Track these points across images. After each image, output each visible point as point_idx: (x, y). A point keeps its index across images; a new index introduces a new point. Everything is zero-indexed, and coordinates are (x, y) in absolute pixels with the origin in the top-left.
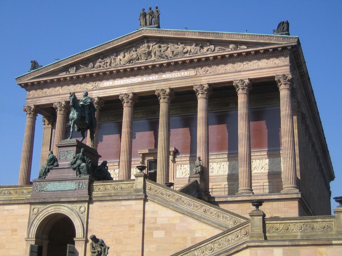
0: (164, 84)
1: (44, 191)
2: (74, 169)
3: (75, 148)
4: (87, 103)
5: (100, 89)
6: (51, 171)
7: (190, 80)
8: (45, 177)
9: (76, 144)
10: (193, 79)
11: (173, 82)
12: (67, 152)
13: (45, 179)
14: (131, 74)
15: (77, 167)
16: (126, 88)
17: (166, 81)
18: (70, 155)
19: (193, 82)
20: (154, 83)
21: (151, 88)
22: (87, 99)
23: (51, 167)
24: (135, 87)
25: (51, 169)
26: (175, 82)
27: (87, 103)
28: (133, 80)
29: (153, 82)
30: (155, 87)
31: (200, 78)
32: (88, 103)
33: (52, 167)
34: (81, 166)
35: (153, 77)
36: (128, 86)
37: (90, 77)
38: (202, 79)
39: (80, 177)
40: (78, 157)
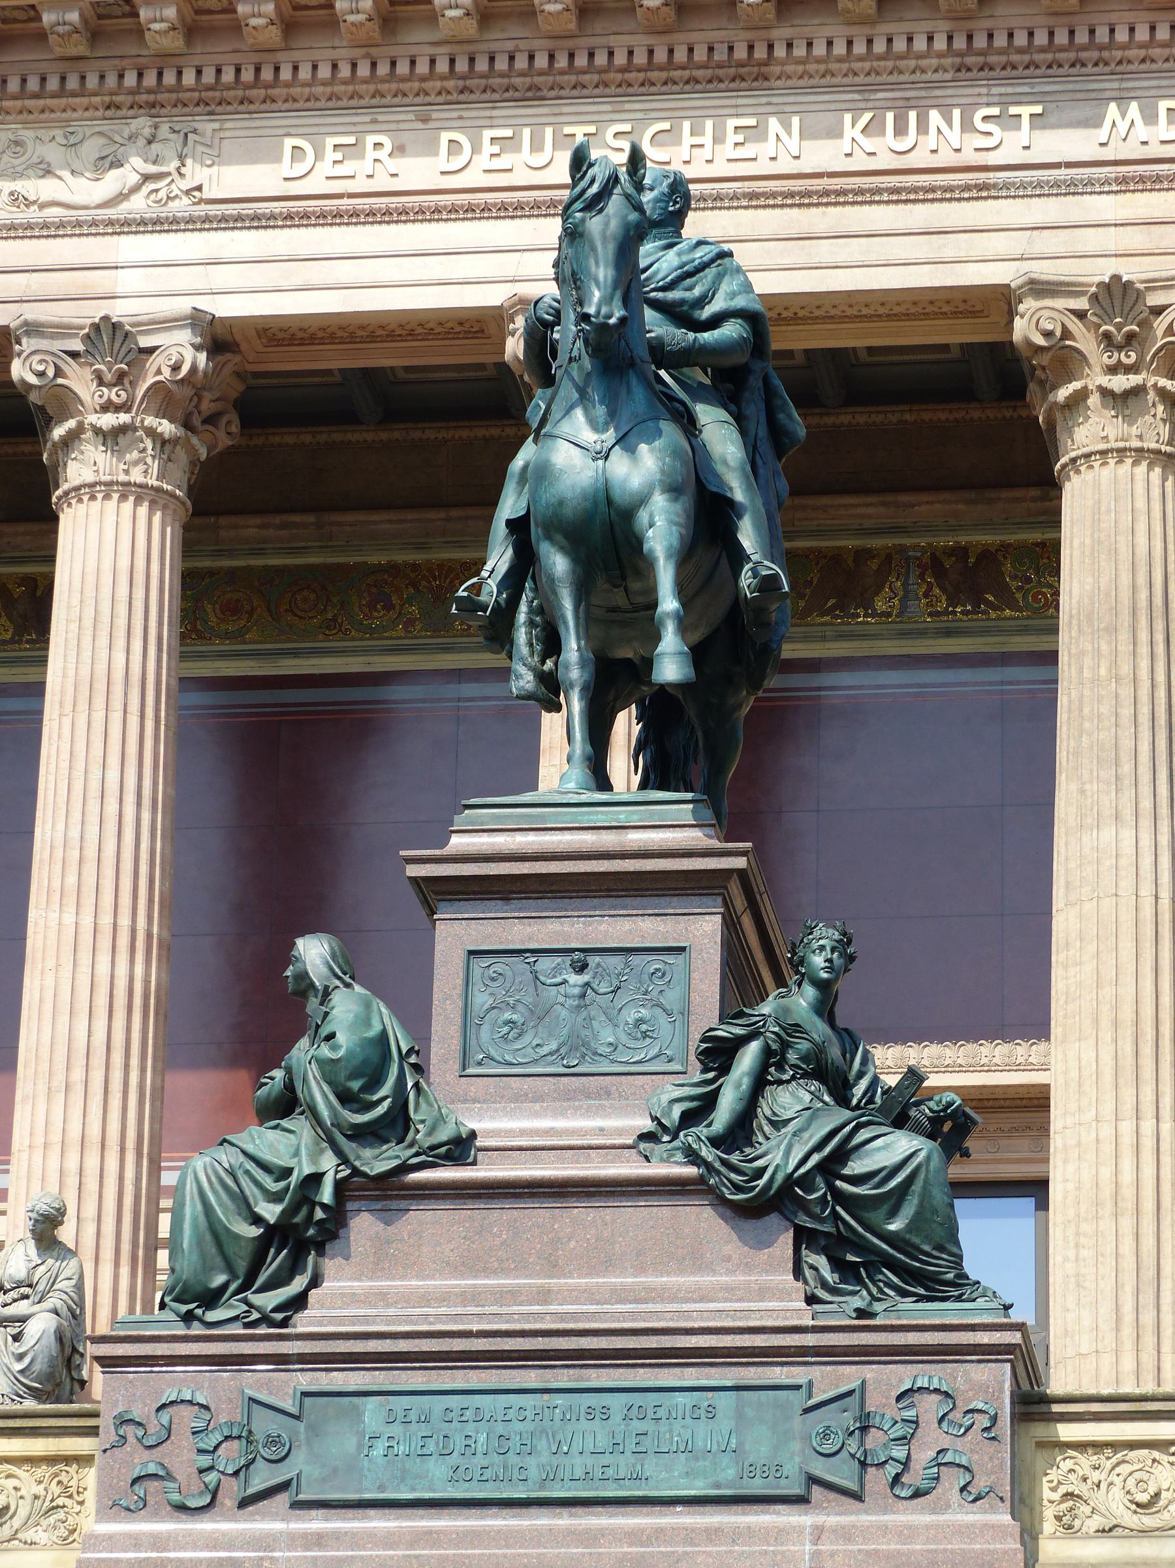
0: (1123, 214)
1: (297, 1505)
2: (756, 1207)
3: (703, 931)
4: (715, 322)
5: (215, 210)
6: (363, 1225)
8: (299, 1302)
9: (740, 863)
12: (581, 968)
13: (303, 1322)
14: (661, 56)
15: (806, 1182)
18: (631, 1015)
20: (983, 192)
22: (710, 273)
23: (377, 1160)
25: (390, 1191)
27: (715, 322)
28: (687, 140)
32: (731, 330)
33: (404, 1168)
34: (855, 1167)
37: (82, 50)
39: (861, 1313)
40: (785, 1045)
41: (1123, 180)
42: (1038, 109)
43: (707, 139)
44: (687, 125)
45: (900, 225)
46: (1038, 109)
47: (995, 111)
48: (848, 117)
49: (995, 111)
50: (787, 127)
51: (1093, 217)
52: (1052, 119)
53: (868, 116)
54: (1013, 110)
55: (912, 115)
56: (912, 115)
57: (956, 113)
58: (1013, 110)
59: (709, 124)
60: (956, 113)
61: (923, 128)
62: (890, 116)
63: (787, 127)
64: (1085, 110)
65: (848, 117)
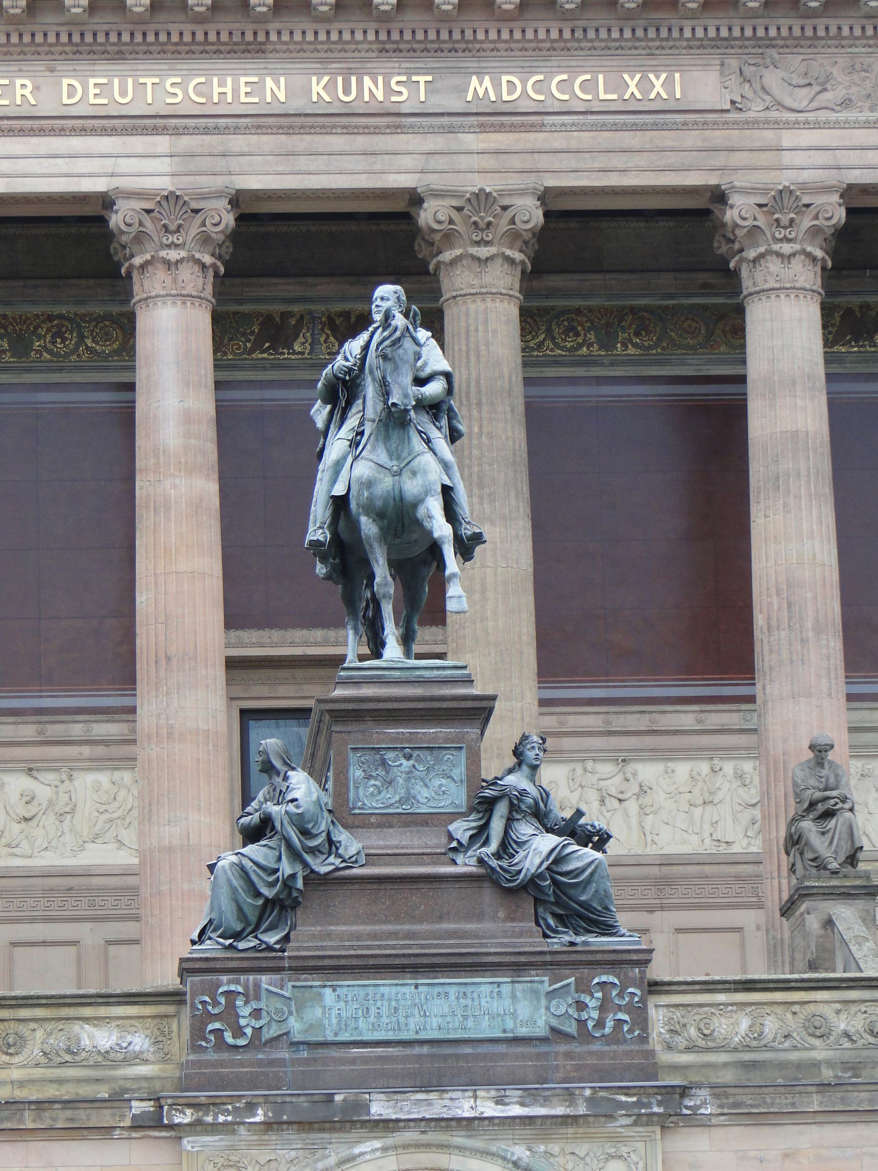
0: (482, 146)
7: (691, 138)
10: (718, 137)
11: (558, 141)
16: (162, 143)
17: (500, 128)
19: (721, 159)
20: (397, 129)
21: (378, 167)
24: (238, 142)
26: (574, 145)
28: (216, 90)
29: (393, 119)
30: (408, 162)
31: (769, 136)
35: (387, 84)
36: (177, 132)
38: (786, 144)
41: (481, 125)
42: (430, 78)
43: (228, 90)
44: (215, 80)
45: (347, 148)
46: (430, 78)
47: (404, 78)
48: (314, 79)
49: (404, 78)
50: (277, 83)
51: (464, 147)
52: (437, 85)
53: (326, 79)
54: (414, 78)
55: (354, 79)
56: (354, 79)
57: (380, 79)
58: (414, 78)
59: (229, 80)
60: (380, 79)
61: (360, 84)
62: (340, 79)
63: (277, 83)
64: (456, 80)
65: (314, 79)
